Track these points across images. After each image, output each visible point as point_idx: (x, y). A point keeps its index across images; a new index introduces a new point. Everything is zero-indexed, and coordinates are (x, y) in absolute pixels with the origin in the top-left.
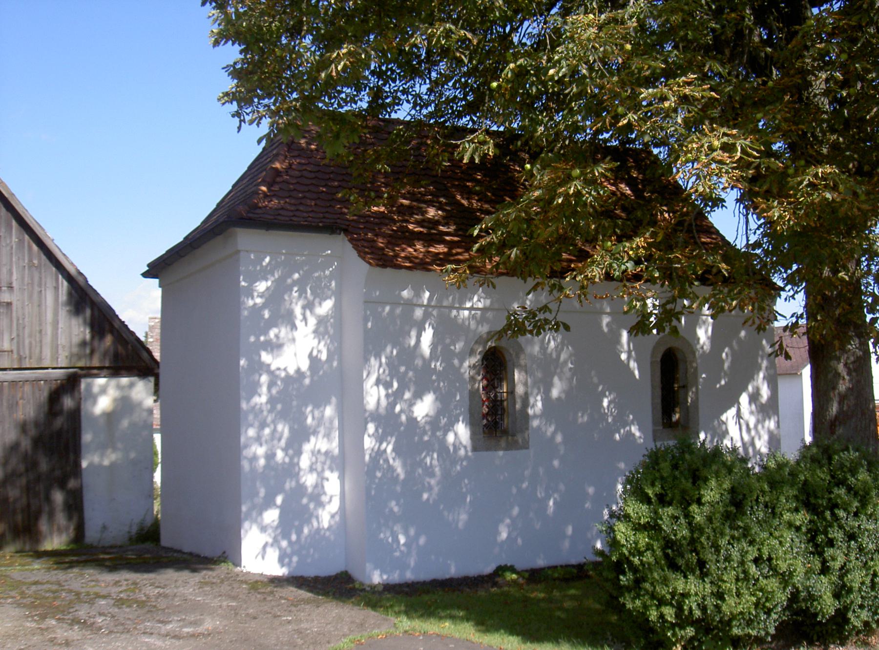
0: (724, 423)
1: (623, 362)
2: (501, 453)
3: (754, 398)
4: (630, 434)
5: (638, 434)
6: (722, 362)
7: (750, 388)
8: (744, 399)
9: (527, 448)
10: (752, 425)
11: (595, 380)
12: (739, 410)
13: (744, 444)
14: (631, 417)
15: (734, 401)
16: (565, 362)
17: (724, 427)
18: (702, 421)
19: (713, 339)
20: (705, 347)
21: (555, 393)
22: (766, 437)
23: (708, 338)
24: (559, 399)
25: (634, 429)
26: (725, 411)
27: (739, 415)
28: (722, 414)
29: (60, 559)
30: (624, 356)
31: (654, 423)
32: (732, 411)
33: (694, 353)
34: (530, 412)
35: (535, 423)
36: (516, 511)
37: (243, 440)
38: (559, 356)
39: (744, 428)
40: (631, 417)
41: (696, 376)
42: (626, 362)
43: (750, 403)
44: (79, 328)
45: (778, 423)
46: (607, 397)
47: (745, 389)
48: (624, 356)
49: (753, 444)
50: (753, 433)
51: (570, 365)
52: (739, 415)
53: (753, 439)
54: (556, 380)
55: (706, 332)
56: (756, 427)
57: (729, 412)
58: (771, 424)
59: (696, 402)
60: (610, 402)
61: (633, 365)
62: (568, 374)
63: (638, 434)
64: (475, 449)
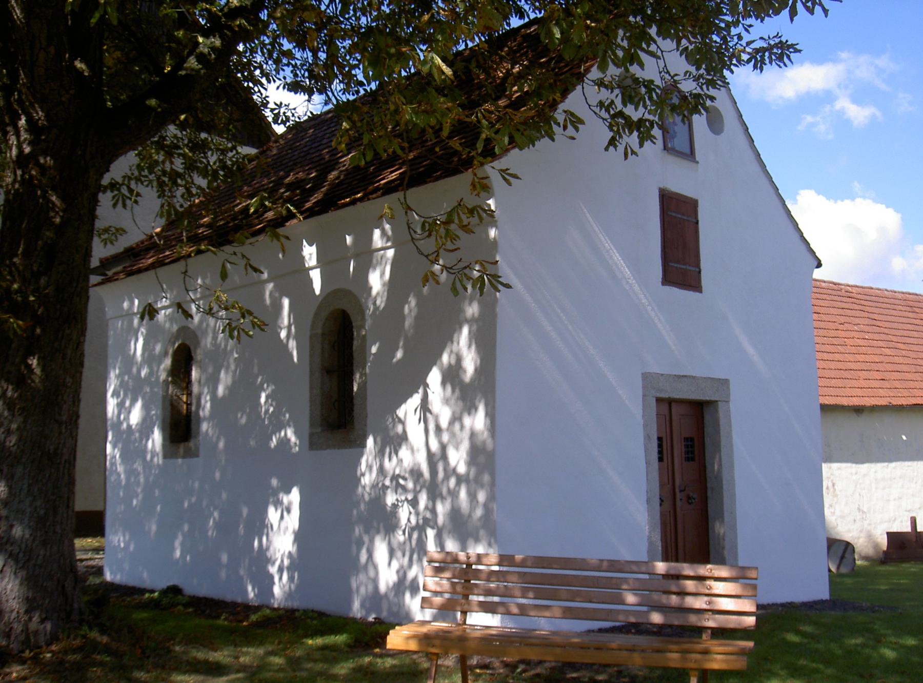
0: (400, 421)
1: (282, 341)
2: (180, 461)
3: (452, 376)
4: (285, 442)
5: (293, 439)
6: (403, 318)
7: (445, 358)
8: (434, 377)
9: (197, 456)
10: (444, 424)
11: (256, 370)
12: (425, 396)
13: (430, 455)
14: (287, 416)
15: (418, 382)
16: (231, 352)
17: (400, 429)
18: (370, 420)
19: (392, 286)
20: (378, 302)
21: (221, 391)
22: (465, 446)
23: (384, 285)
24: (224, 396)
25: (290, 433)
26: (404, 400)
27: (425, 406)
28: (399, 406)
29: (634, 634)
30: (283, 334)
31: (312, 425)
32: (415, 400)
33: (362, 311)
34: (201, 413)
35: (204, 426)
36: (186, 528)
37: (359, 473)
38: (226, 346)
39: (432, 427)
40: (287, 416)
41: (365, 350)
42: (285, 341)
43: (444, 383)
44: (168, 376)
45: (491, 415)
46: (265, 391)
47: (434, 359)
48: (283, 334)
49: (444, 456)
50: (445, 437)
51: (236, 356)
52: (425, 406)
53: (443, 448)
54: (222, 374)
55: (382, 274)
56: (451, 423)
57: (410, 401)
58: (478, 421)
59: (363, 386)
60: (267, 397)
61: (292, 344)
62: (233, 367)
63: (293, 439)
64: (165, 456)
